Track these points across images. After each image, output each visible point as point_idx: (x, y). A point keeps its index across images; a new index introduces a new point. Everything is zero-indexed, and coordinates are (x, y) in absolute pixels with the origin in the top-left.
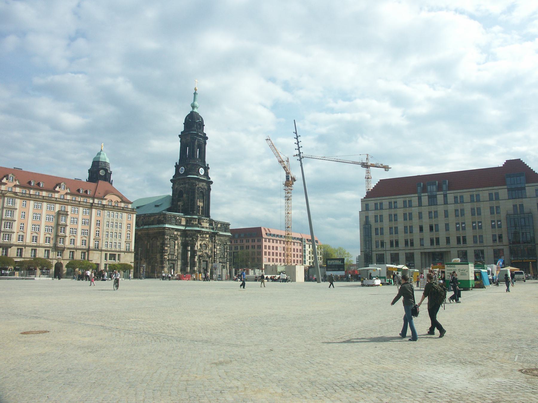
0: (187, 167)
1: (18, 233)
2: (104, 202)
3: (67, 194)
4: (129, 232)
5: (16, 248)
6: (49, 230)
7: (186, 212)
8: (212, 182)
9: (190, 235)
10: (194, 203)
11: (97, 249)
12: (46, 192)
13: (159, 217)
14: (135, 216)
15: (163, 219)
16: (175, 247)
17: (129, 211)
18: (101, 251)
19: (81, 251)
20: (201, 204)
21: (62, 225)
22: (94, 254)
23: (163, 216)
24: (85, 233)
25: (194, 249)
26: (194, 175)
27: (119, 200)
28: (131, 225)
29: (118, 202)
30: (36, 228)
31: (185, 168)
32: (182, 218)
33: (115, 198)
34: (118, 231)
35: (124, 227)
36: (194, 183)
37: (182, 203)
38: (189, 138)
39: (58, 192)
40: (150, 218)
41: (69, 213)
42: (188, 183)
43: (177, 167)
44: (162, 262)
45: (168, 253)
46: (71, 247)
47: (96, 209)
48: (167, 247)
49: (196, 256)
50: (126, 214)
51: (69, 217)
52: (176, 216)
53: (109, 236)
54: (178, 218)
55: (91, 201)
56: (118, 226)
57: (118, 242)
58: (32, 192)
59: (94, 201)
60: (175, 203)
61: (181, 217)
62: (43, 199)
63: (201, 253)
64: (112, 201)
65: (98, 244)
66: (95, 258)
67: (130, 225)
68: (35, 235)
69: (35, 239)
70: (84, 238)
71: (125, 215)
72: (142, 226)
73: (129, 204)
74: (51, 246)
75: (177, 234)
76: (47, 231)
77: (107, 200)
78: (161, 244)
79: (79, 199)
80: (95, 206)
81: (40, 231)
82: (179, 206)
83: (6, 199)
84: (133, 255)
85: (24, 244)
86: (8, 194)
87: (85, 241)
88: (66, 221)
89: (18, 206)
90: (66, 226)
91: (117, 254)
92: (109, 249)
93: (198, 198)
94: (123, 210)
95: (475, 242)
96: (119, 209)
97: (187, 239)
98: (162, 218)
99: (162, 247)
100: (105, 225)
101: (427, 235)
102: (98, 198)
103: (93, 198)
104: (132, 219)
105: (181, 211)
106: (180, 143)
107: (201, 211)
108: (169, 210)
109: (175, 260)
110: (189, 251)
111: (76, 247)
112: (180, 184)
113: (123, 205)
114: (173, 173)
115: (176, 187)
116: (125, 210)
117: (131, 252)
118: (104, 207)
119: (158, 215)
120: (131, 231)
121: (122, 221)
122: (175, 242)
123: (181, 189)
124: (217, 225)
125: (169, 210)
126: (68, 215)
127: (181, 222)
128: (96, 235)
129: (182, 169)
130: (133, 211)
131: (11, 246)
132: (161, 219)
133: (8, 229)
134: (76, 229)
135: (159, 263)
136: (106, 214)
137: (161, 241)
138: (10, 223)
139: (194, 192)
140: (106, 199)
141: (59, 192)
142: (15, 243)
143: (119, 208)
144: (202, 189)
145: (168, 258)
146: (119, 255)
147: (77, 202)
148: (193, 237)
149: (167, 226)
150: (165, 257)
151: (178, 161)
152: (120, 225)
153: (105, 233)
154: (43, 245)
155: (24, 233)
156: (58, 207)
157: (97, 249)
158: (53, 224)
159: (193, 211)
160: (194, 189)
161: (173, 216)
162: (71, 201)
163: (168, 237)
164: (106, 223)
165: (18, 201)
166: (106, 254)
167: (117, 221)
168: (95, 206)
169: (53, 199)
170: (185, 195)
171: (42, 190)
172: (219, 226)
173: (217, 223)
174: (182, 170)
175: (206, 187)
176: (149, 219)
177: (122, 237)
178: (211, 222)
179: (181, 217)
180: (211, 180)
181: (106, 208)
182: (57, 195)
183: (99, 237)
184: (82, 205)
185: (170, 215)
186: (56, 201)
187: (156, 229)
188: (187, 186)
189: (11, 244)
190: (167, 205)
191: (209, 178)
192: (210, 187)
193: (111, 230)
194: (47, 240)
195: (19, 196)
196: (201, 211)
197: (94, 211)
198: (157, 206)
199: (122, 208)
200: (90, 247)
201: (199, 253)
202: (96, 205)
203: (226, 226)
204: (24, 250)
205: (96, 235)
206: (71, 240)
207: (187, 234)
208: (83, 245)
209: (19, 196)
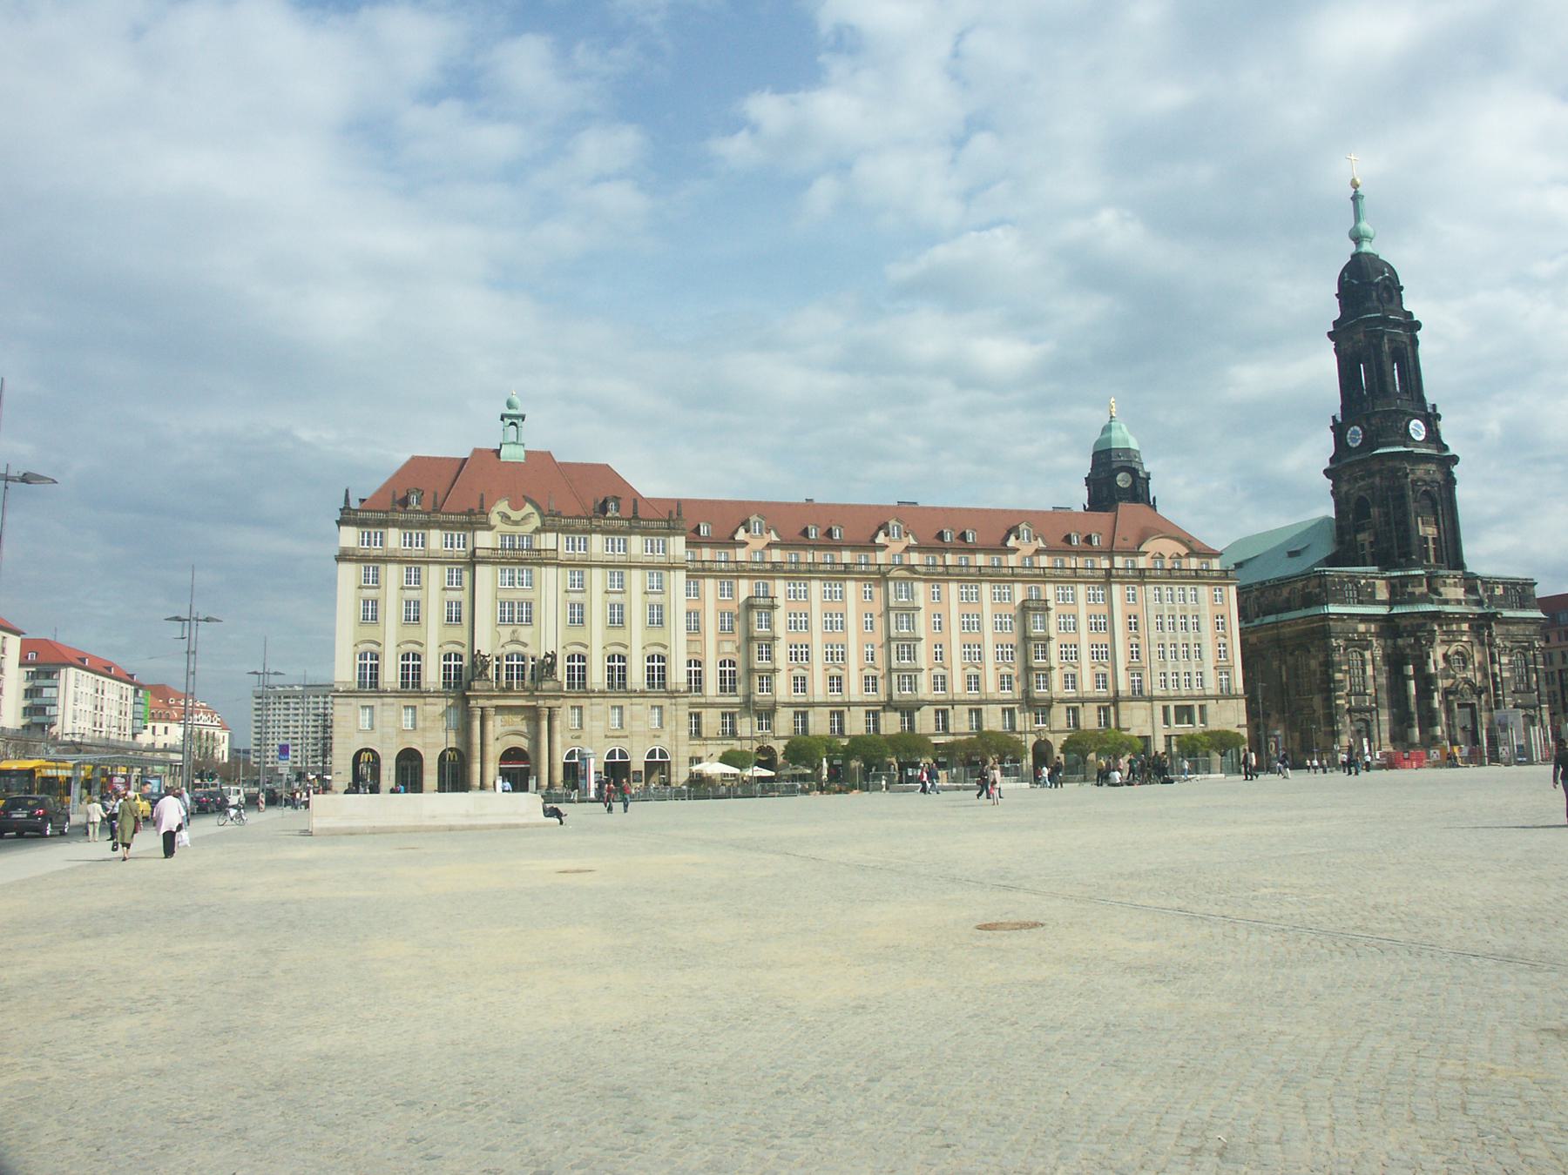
1: (930, 669)
2: (1142, 562)
3: (1038, 552)
4: (1222, 640)
5: (791, 711)
6: (835, 656)
7: (1385, 562)
8: (1454, 459)
9: (1409, 628)
10: (1407, 530)
11: (1138, 695)
12: (985, 554)
13: (1305, 586)
14: (1233, 590)
15: (1317, 590)
16: (1364, 671)
17: (1215, 578)
18: (1151, 699)
19: (1095, 705)
20: (1431, 531)
21: (1039, 638)
22: (1132, 709)
23: (1315, 582)
24: (799, 656)
25: (1424, 670)
26: (1398, 444)
27: (1183, 551)
28: (1227, 617)
29: (1179, 556)
30: (974, 653)
31: (1362, 428)
32: (1377, 582)
33: (1169, 547)
34: (1192, 639)
35: (1207, 625)
36: (1400, 469)
39: (1014, 550)
40: (1278, 591)
41: (1051, 604)
43: (1339, 430)
44: (1331, 719)
45: (1346, 691)
46: (1069, 696)
47: (1120, 583)
48: (1340, 671)
49: (1433, 691)
50: (1206, 588)
51: (1052, 613)
52: (1355, 577)
53: (1168, 655)
54: (1363, 582)
55: (1106, 564)
56: (1190, 626)
57: (1194, 670)
58: (950, 559)
59: (1112, 562)
60: (1348, 538)
61: (1372, 578)
62: (981, 575)
63: (1451, 681)
64: (1162, 556)
65: (1140, 681)
66: (1138, 721)
67: (1135, 617)
68: (973, 671)
69: (974, 682)
70: (1101, 669)
71: (1204, 591)
72: (1258, 617)
73: (1211, 558)
74: (882, 699)
75: (1368, 631)
76: (832, 659)
77: (1150, 555)
78: (1321, 665)
79: (1071, 562)
80: (1118, 576)
81: (810, 659)
82: (1363, 545)
83: (891, 584)
84: (1242, 703)
85: (950, 697)
86: (895, 573)
87: (1104, 675)
88: (1045, 626)
89: (920, 600)
90: (1049, 639)
91: (1196, 704)
92: (1172, 694)
93: (1417, 515)
94: (1197, 576)
96: (1186, 577)
97: (1400, 642)
98: (1314, 588)
99: (1326, 673)
100: (1153, 626)
102: (1122, 553)
103: (1110, 554)
104: (1225, 600)
105: (1368, 559)
107: (1432, 553)
108: (1332, 561)
109: (1370, 710)
110: (1410, 678)
111: (1081, 695)
112: (1356, 480)
113: (1194, 563)
114: (1331, 451)
115: (1344, 488)
116: (1203, 577)
117: (1236, 697)
118: (1145, 577)
119: (1301, 580)
120: (1228, 635)
121: (1198, 610)
122: (1362, 656)
123: (1362, 493)
124: (1493, 590)
125: (1332, 561)
126: (1048, 609)
127: (1373, 594)
128: (1133, 658)
129: (1355, 432)
130: (1227, 577)
131: (918, 705)
132: (1313, 590)
133: (906, 661)
134: (1075, 646)
135: (1322, 722)
136: (1151, 596)
137: (1321, 658)
138: (909, 646)
139: (1401, 498)
140: (1145, 553)
141: (1018, 550)
142: (929, 698)
143: (1184, 573)
144: (1426, 483)
145: (1347, 706)
146: (1202, 707)
147: (1068, 572)
148: (1419, 634)
149: (1333, 609)
150: (1338, 702)
151: (1337, 411)
152: (1195, 620)
153: (1155, 649)
154: (998, 696)
155: (944, 668)
156: (1019, 592)
157: (1138, 695)
158: (1012, 637)
159: (1406, 555)
160: (1402, 488)
161: (1347, 577)
162: (1053, 571)
163: (1341, 642)
164: (1153, 621)
165: (920, 587)
166: (1165, 709)
167: (1185, 609)
168: (1118, 576)
169: (1005, 571)
170: (1374, 511)
171: (973, 551)
172: (1499, 591)
173: (1489, 583)
174: (1355, 436)
175: (1439, 477)
176: (1275, 594)
177: (1204, 656)
178: (1471, 583)
179: (1372, 578)
180: (1452, 451)
181: (1150, 577)
182: (1012, 560)
183: (1141, 661)
184: (1084, 577)
185: (1339, 577)
186: (1014, 577)
187: (1300, 621)
188: (1377, 480)
189: (918, 701)
190: (1326, 549)
191: (1446, 448)
192: (1450, 473)
193: (1171, 638)
194: (1005, 681)
195: (919, 573)
196: (1432, 553)
197: (1116, 588)
198: (1292, 554)
199: (1193, 574)
200: (1118, 691)
201: (1442, 683)
202: (1121, 573)
203: (1523, 590)
204: (951, 713)
205: (1133, 658)
206: (1066, 676)
208: (1098, 687)
209: (919, 573)
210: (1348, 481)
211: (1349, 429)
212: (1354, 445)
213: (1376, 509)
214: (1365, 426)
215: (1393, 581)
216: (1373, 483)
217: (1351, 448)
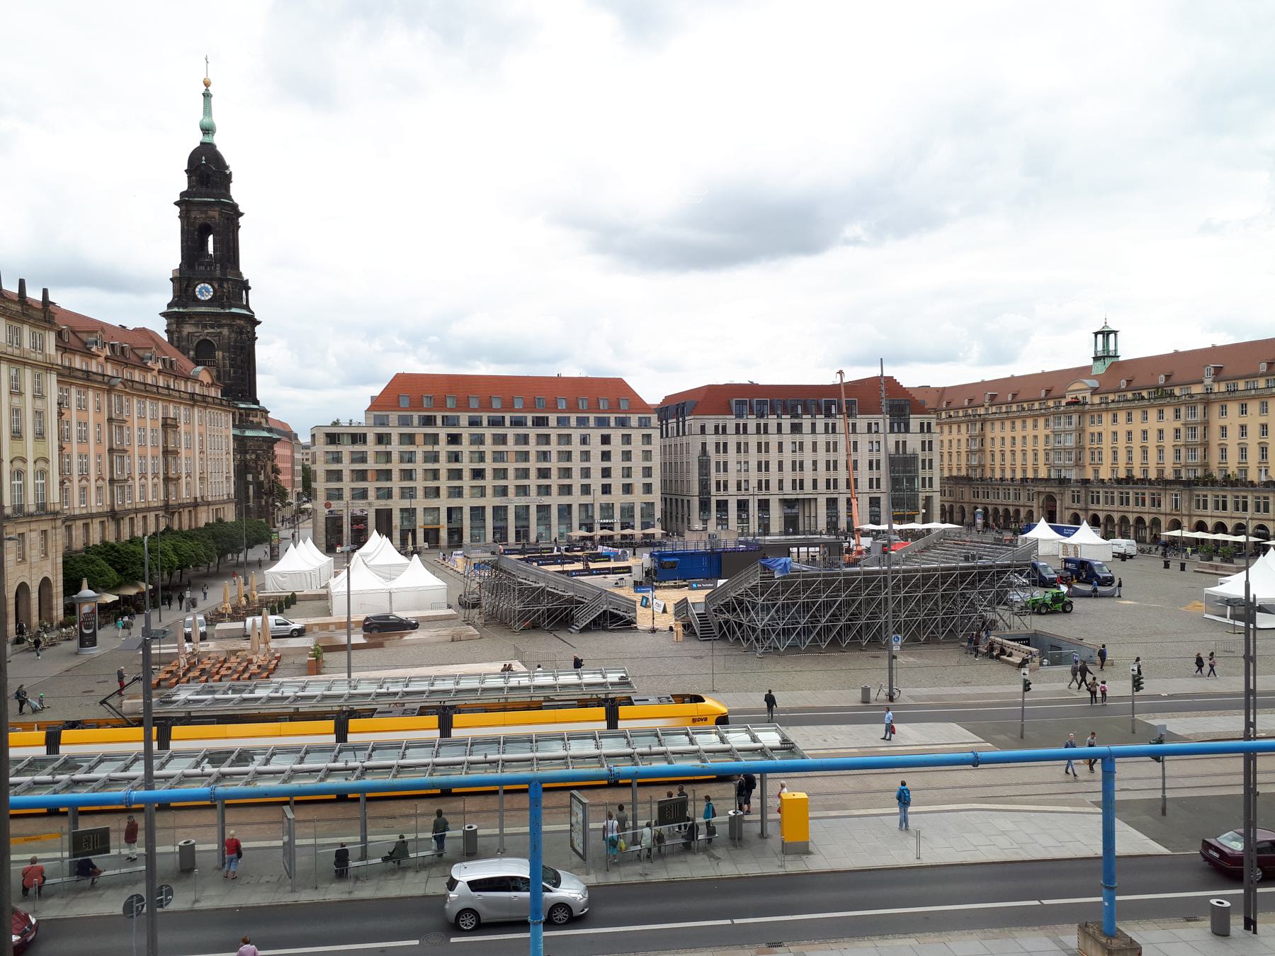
38: (216, 214)
95: (739, 488)
97: (248, 457)
101: (788, 476)
106: (178, 223)
112: (205, 326)
123: (208, 338)
170: (219, 354)
188: (225, 331)
207: (245, 445)
211: (197, 285)
213: (221, 353)
215: (242, 411)
216: (220, 333)
217: (199, 300)
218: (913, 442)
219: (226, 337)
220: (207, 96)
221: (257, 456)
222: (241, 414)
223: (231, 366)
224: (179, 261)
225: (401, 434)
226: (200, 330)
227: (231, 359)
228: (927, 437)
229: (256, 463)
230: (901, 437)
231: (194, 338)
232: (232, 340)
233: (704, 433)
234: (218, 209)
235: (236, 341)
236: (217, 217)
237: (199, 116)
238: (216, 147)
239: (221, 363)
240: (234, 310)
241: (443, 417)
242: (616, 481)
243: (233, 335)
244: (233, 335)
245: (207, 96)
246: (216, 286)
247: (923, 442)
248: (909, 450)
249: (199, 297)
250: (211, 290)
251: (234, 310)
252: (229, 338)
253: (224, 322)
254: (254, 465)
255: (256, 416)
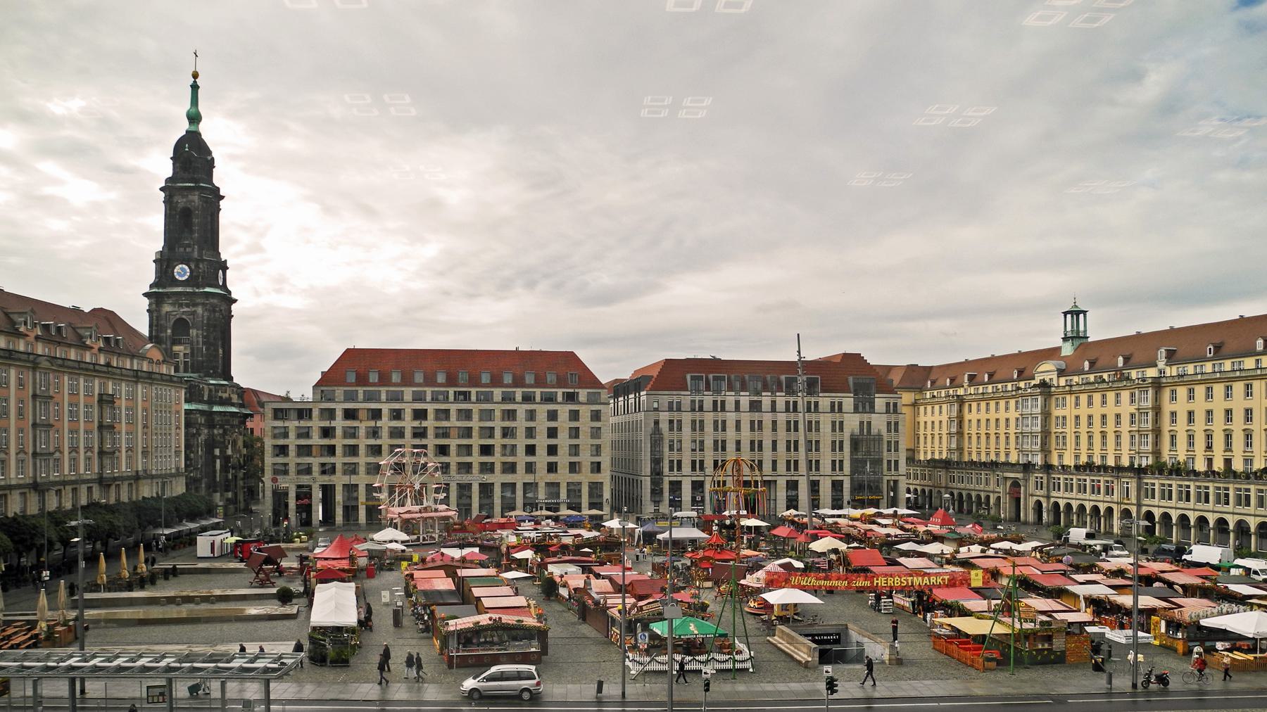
0: (199, 268)
31: (190, 268)
37: (185, 349)
38: (196, 198)
42: (203, 304)
43: (164, 263)
97: (216, 431)
112: (181, 305)
123: (184, 317)
170: (193, 332)
174: (182, 272)
188: (200, 310)
207: (213, 420)
210: (172, 304)
211: (177, 265)
212: (180, 279)
214: (193, 267)
216: (195, 311)
218: (879, 422)
219: (200, 316)
220: (195, 87)
221: (225, 431)
222: (210, 390)
223: (204, 343)
224: (162, 244)
225: (481, 410)
226: (176, 309)
227: (204, 337)
228: (893, 418)
229: (224, 438)
230: (865, 417)
231: (171, 317)
232: (205, 318)
233: (775, 411)
234: (197, 193)
235: (209, 319)
236: (197, 201)
237: (188, 106)
238: (200, 134)
239: (195, 340)
240: (208, 290)
241: (477, 392)
242: (585, 458)
243: (206, 314)
244: (206, 314)
245: (195, 87)
246: (193, 267)
247: (889, 424)
248: (874, 431)
249: (177, 277)
250: (188, 270)
251: (208, 290)
252: (203, 316)
253: (199, 301)
254: (222, 440)
255: (226, 392)
